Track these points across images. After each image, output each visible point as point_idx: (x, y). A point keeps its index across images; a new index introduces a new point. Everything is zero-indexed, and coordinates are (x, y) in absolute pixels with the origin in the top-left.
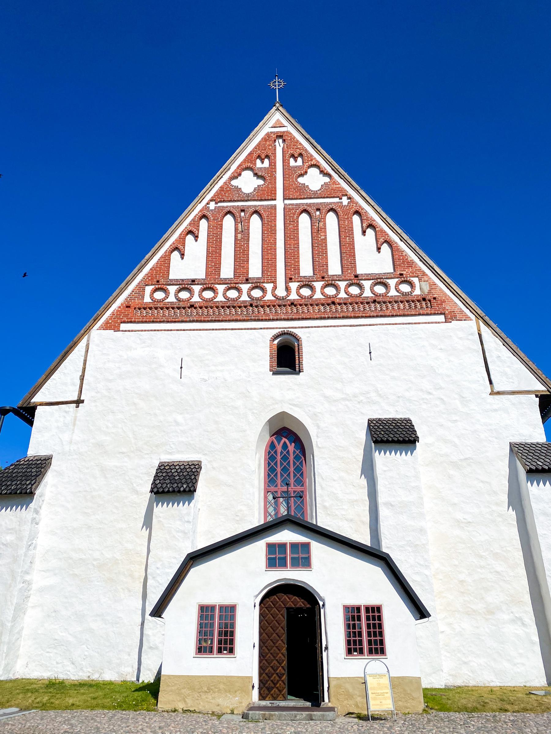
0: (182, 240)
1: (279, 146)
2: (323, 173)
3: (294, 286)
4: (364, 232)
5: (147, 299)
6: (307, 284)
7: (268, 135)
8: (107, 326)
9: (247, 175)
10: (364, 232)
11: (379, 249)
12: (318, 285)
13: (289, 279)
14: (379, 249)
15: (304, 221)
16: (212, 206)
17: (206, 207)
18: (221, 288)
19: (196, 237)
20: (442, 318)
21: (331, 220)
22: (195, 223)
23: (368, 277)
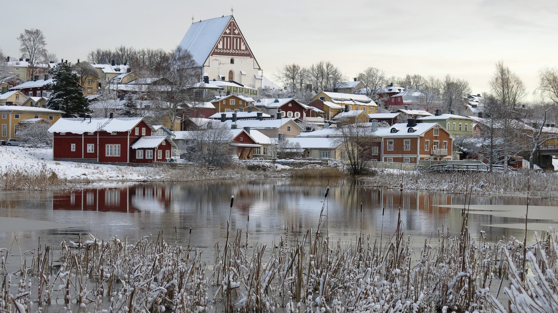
0: (219, 41)
1: (232, 24)
6: (235, 50)
9: (228, 29)
12: (236, 51)
15: (235, 39)
16: (223, 35)
20: (250, 57)
22: (221, 39)
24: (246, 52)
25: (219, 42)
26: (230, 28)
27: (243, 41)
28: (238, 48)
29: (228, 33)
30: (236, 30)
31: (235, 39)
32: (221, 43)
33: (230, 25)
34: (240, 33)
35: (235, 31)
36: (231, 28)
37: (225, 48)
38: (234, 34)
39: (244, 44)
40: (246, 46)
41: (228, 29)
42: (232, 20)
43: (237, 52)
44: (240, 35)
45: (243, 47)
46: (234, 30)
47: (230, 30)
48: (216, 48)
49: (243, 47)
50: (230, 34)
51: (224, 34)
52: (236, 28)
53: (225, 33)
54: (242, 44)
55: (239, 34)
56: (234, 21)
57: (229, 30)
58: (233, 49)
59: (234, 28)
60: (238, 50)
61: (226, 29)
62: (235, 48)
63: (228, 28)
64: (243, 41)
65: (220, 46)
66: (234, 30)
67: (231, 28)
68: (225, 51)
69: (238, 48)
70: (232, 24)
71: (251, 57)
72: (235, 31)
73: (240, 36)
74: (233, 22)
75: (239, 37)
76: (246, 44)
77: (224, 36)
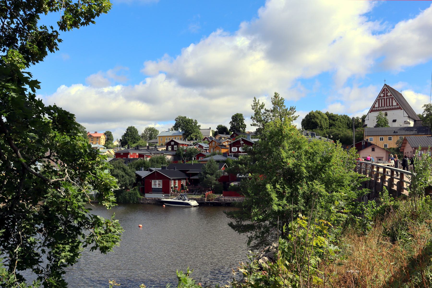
1: (385, 90)
9: (382, 94)
15: (388, 100)
21: (391, 99)
22: (377, 101)
25: (376, 103)
26: (384, 93)
27: (394, 99)
28: (391, 105)
29: (382, 96)
31: (388, 100)
32: (377, 103)
33: (384, 90)
35: (388, 94)
38: (387, 96)
41: (382, 94)
43: (389, 108)
44: (392, 96)
46: (388, 93)
47: (384, 94)
48: (373, 107)
50: (384, 96)
52: (388, 92)
53: (380, 97)
56: (386, 87)
57: (383, 94)
58: (389, 105)
59: (387, 92)
62: (388, 105)
63: (382, 92)
64: (394, 99)
65: (377, 106)
66: (387, 93)
68: (380, 108)
69: (391, 105)
70: (385, 90)
71: (401, 109)
72: (388, 94)
75: (391, 98)
77: (379, 99)
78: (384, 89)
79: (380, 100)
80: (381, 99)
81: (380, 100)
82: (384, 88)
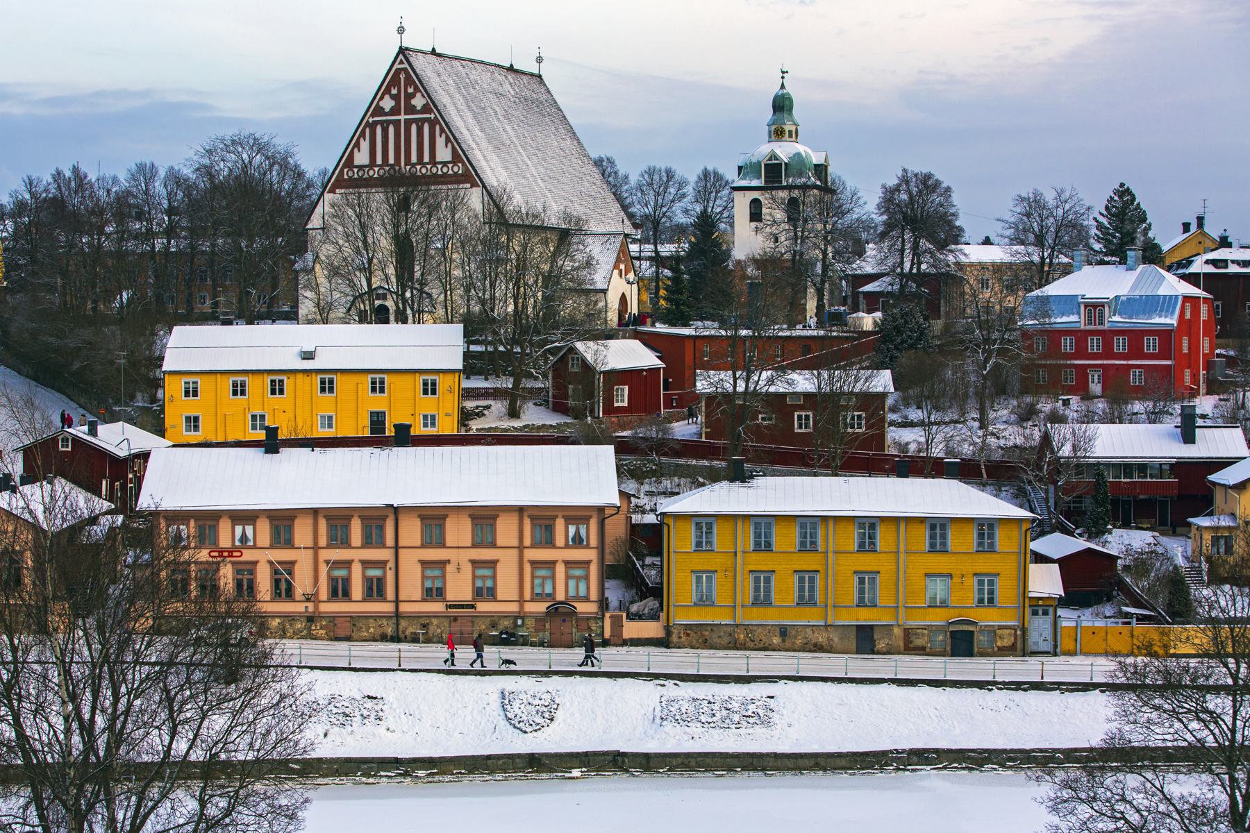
1: (402, 76)
2: (423, 95)
3: (408, 167)
4: (441, 136)
5: (346, 177)
7: (397, 69)
8: (329, 192)
9: (387, 97)
10: (441, 136)
11: (447, 146)
13: (406, 165)
14: (447, 146)
15: (414, 128)
16: (371, 120)
17: (368, 121)
18: (376, 169)
19: (365, 140)
23: (440, 163)
24: (456, 169)
26: (394, 91)
30: (419, 95)
31: (414, 128)
34: (431, 105)
35: (414, 102)
36: (399, 91)
37: (426, 159)
38: (411, 109)
39: (448, 140)
40: (454, 149)
41: (387, 97)
42: (401, 62)
44: (430, 111)
45: (444, 154)
46: (413, 96)
47: (396, 98)
49: (444, 154)
50: (395, 111)
51: (373, 115)
54: (440, 141)
55: (426, 109)
56: (406, 65)
59: (410, 90)
60: (424, 165)
61: (382, 98)
64: (442, 131)
66: (409, 97)
67: (399, 91)
70: (402, 76)
72: (414, 102)
73: (432, 116)
74: (405, 70)
76: (453, 140)
77: (376, 123)
78: (398, 71)
79: (379, 130)
80: (381, 123)
81: (379, 130)
82: (397, 66)
